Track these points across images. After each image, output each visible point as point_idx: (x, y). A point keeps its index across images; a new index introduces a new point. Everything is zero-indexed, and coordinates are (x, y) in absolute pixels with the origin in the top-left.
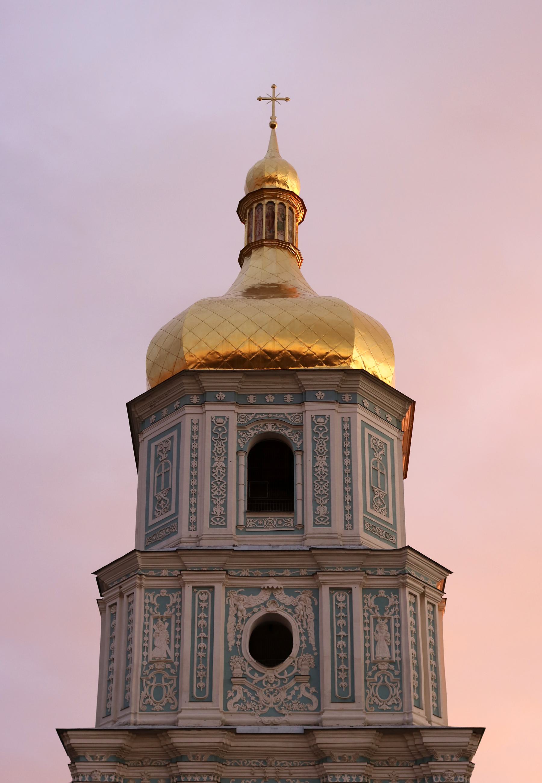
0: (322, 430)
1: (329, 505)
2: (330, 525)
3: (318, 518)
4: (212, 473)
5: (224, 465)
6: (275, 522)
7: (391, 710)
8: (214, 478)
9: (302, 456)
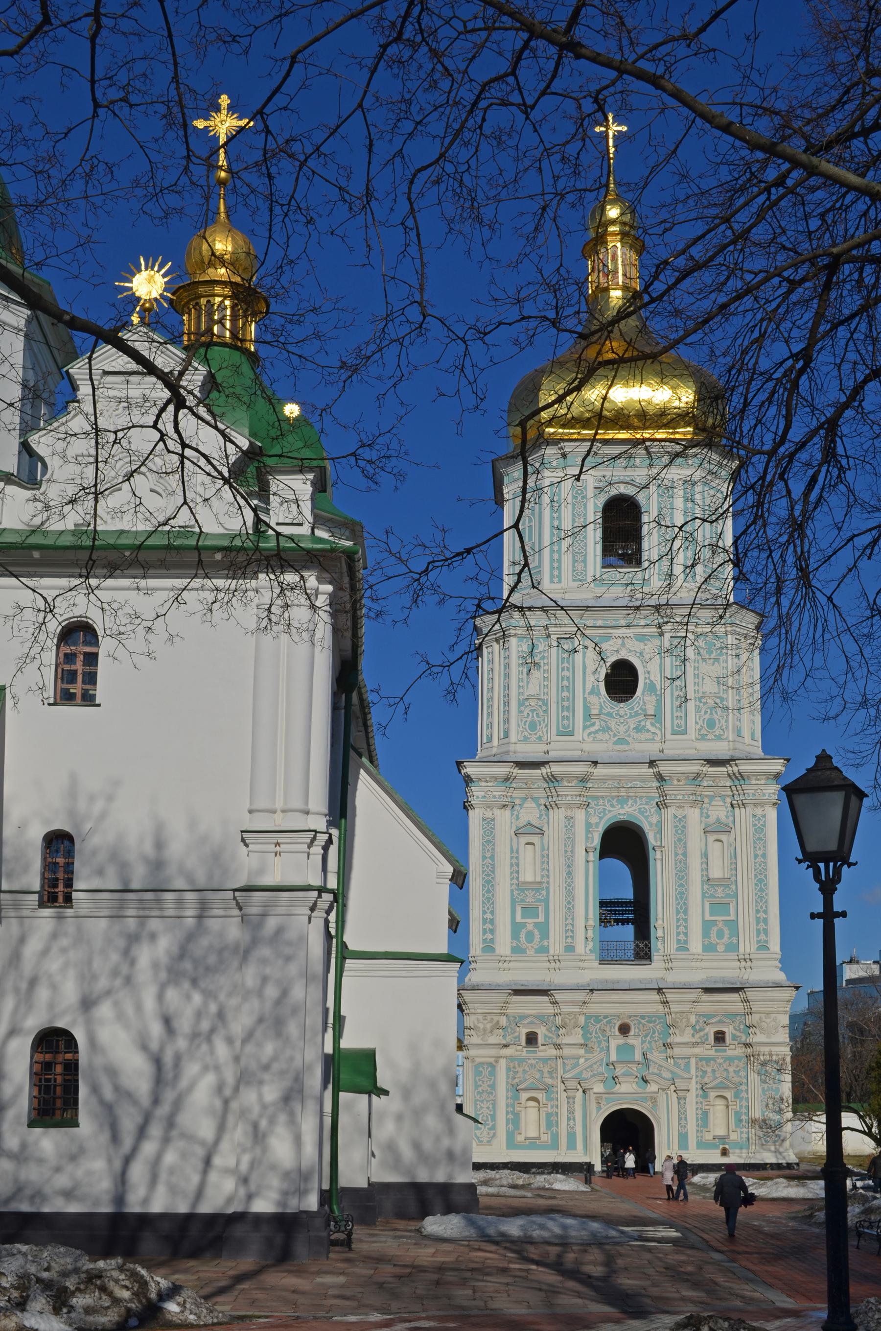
7: (719, 738)
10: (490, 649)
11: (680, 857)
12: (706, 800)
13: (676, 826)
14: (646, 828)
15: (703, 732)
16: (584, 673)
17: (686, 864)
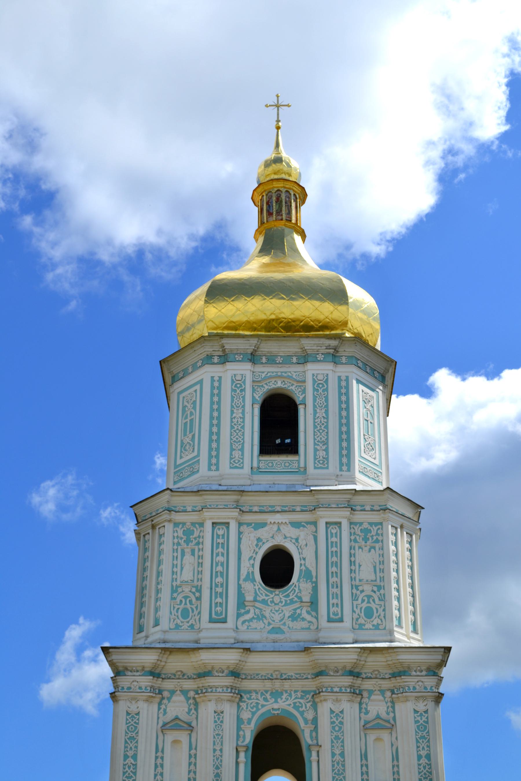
0: (322, 387)
1: (326, 450)
2: (327, 468)
3: (319, 461)
4: (232, 422)
5: (241, 415)
6: (283, 464)
7: (377, 627)
8: (234, 427)
9: (305, 408)
10: (147, 536)
11: (338, 758)
12: (365, 694)
13: (333, 723)
14: (302, 724)
15: (361, 621)
16: (239, 559)
17: (343, 766)
